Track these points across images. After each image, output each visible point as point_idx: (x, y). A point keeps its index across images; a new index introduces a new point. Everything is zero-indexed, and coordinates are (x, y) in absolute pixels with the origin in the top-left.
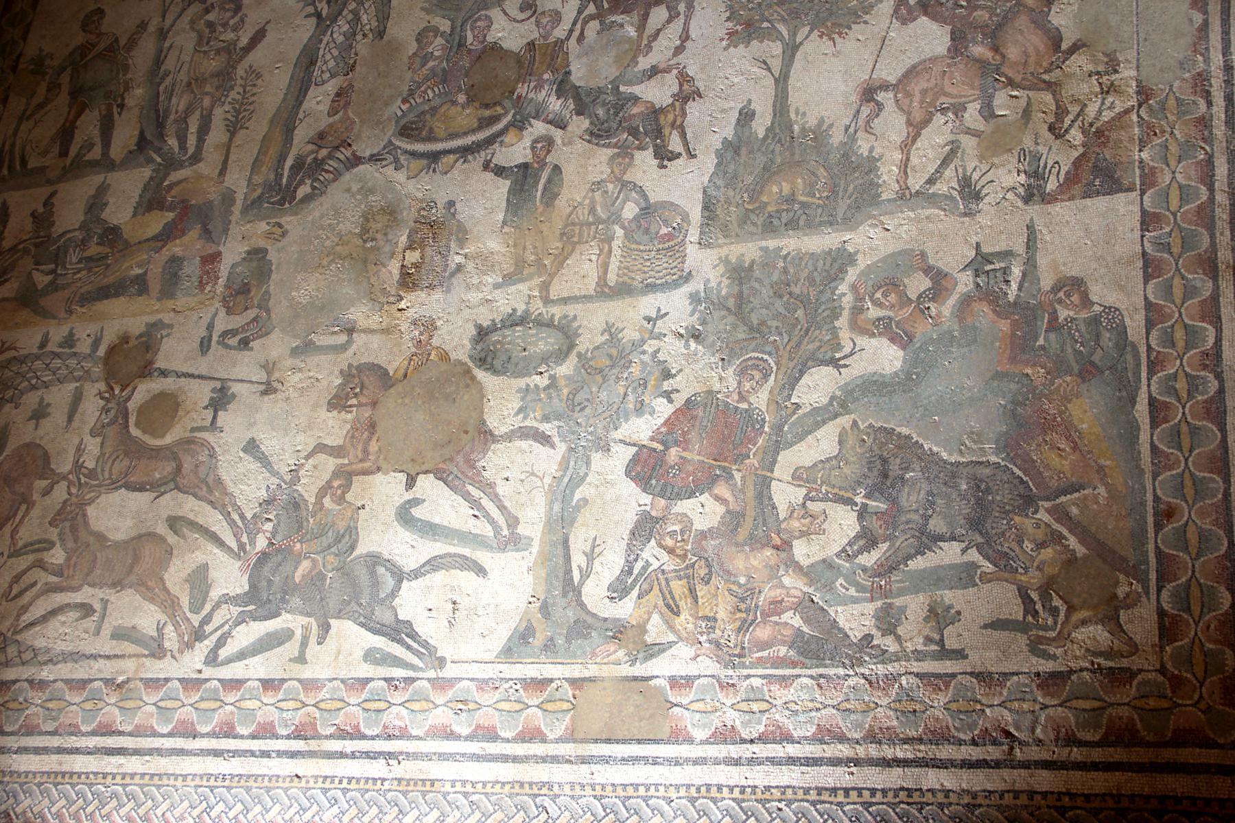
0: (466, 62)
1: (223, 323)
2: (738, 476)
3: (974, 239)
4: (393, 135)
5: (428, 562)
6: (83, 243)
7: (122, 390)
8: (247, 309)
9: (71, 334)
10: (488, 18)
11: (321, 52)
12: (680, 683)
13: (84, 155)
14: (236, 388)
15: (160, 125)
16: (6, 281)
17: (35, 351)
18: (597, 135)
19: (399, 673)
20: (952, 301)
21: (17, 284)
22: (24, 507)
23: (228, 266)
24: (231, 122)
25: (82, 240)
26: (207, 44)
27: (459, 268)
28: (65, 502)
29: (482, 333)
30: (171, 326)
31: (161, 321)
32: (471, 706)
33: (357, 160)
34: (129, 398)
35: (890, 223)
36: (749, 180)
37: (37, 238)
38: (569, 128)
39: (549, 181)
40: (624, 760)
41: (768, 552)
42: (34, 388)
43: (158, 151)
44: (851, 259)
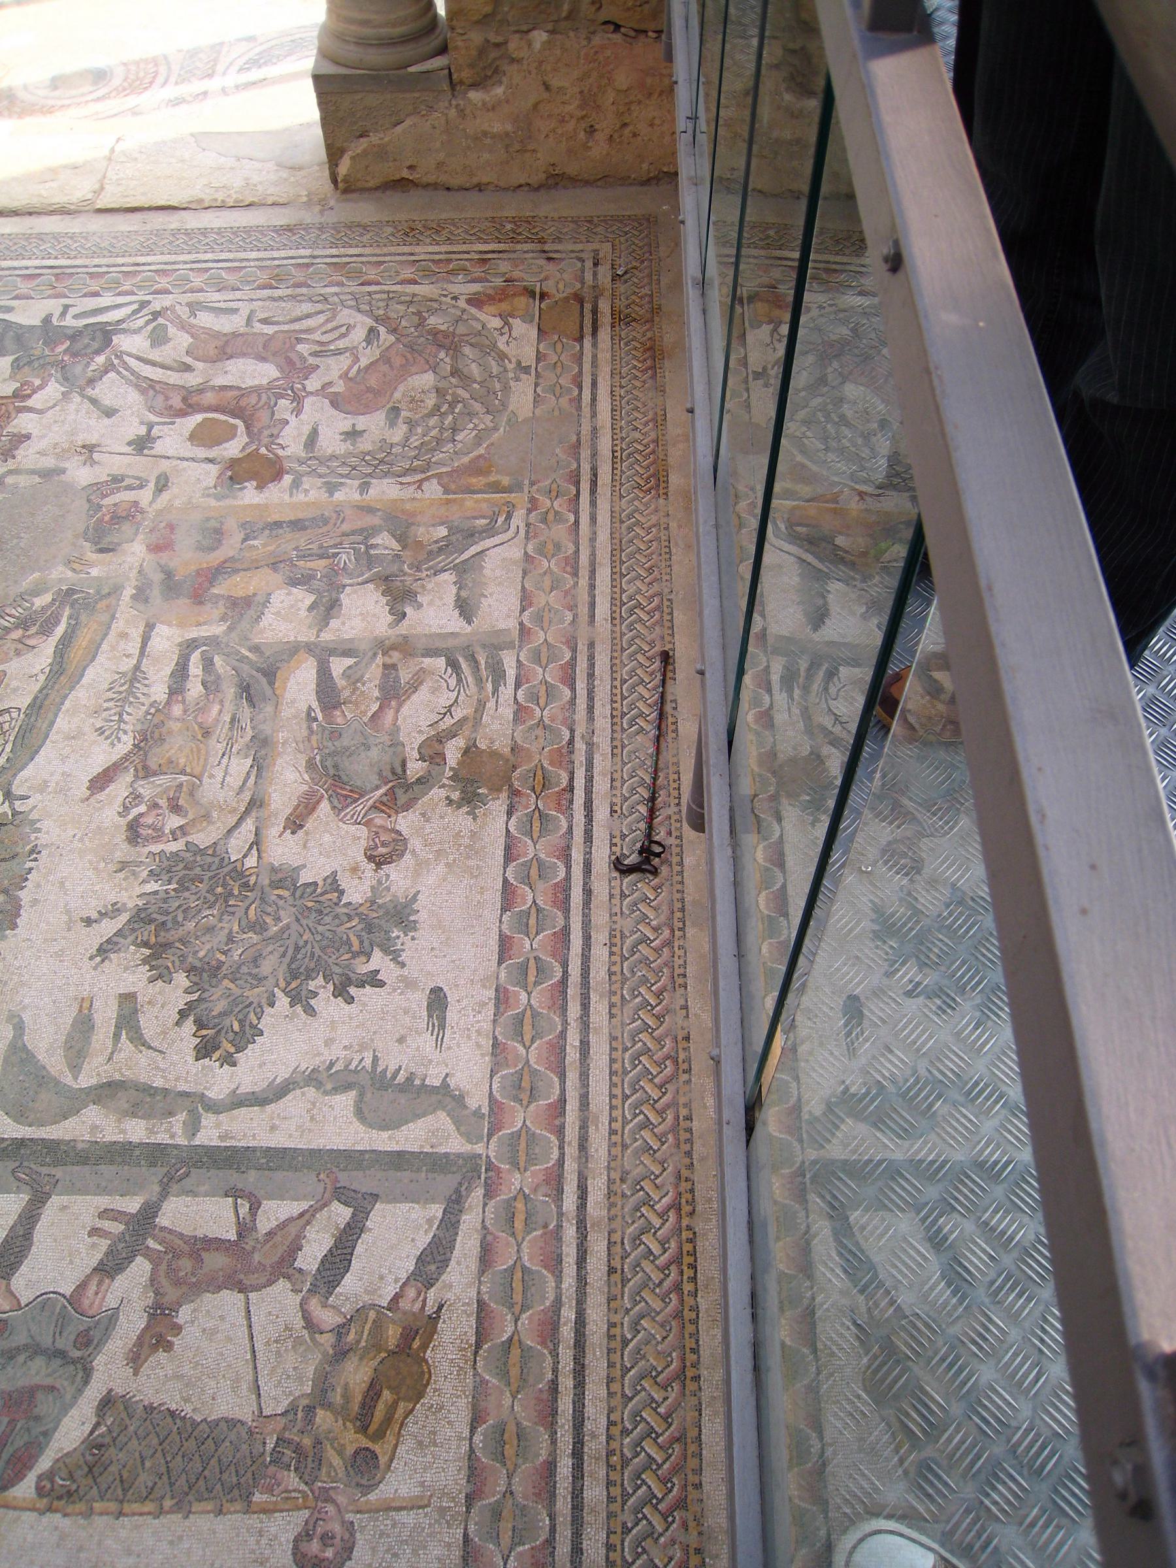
1: (145, 496)
6: (333, 573)
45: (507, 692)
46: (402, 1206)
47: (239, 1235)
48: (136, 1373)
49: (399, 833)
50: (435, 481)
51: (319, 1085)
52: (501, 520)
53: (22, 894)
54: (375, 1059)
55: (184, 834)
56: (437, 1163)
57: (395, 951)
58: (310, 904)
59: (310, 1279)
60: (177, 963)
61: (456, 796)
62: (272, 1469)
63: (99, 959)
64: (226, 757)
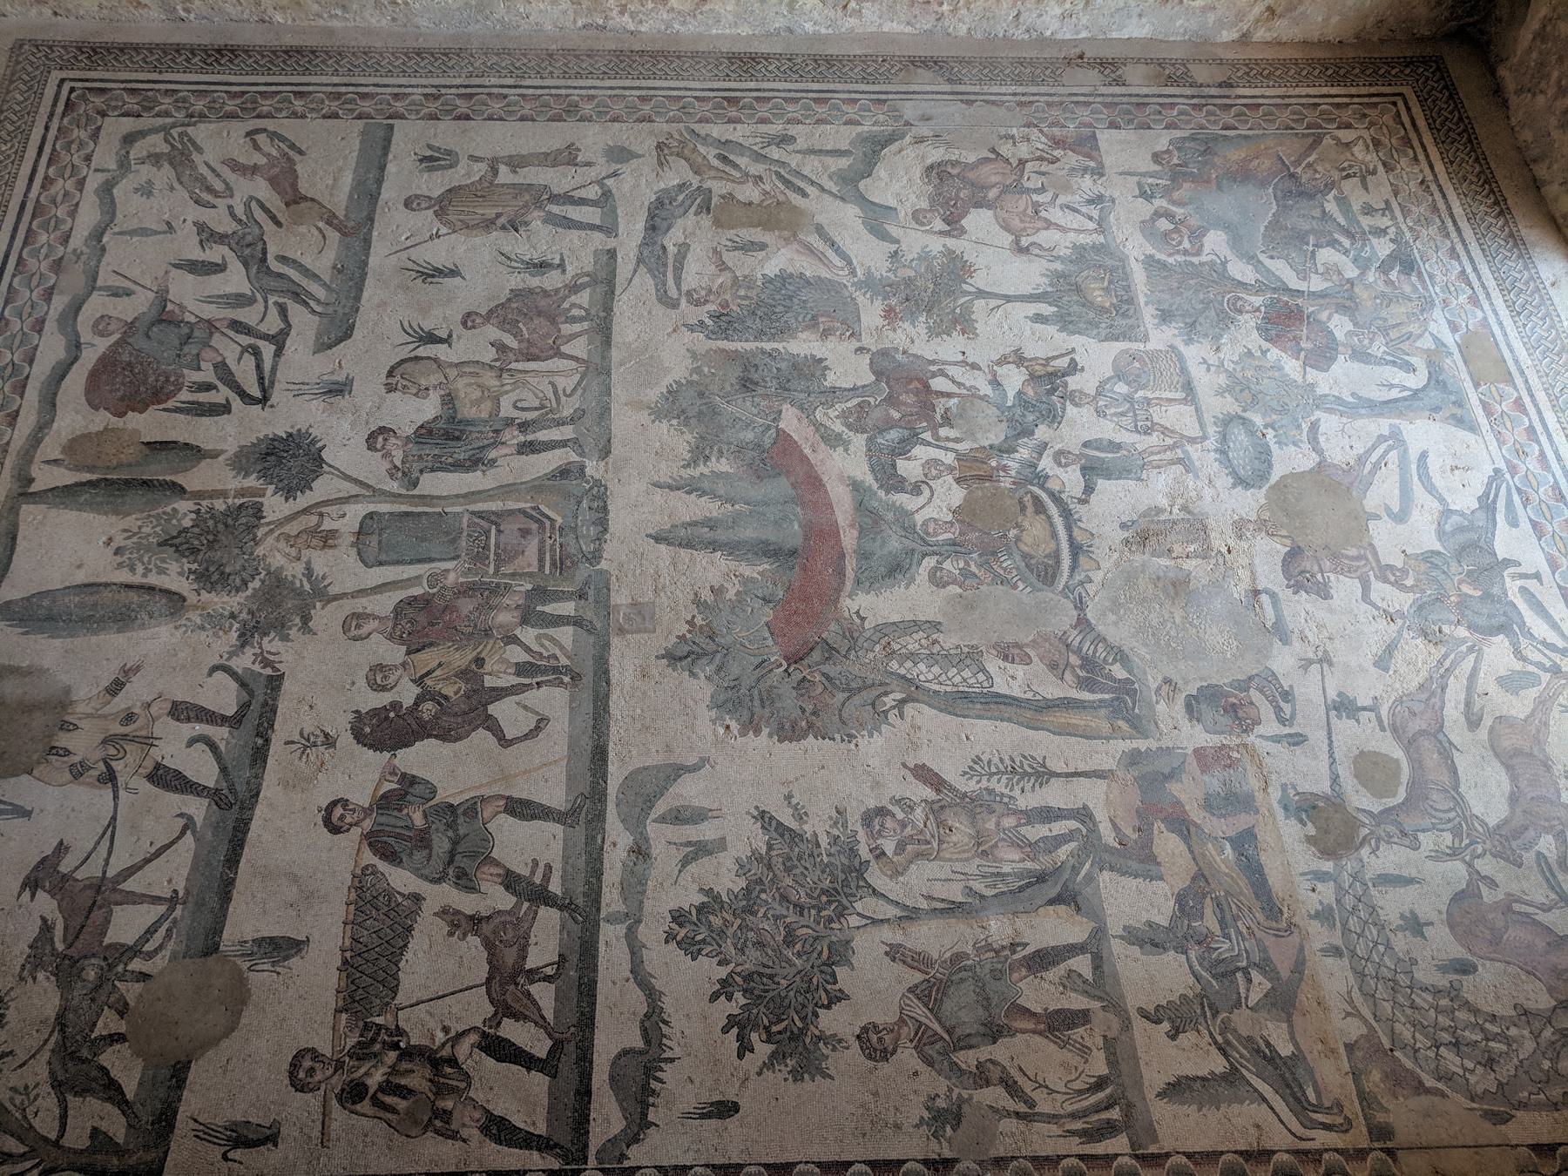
0: (973, 536)
1: (1270, 727)
2: (1311, 309)
3: (1130, 199)
4: (1053, 592)
5: (1430, 493)
7: (1364, 824)
8: (1252, 703)
9: (1317, 916)
10: (925, 523)
11: (949, 689)
12: (1454, 328)
13: (1085, 982)
14: (1332, 694)
15: (1041, 878)
16: (1268, 1044)
17: (1346, 961)
18: (1053, 417)
19: (1516, 498)
20: (1174, 209)
21: (1270, 1025)
22: (1516, 907)
23: (1208, 737)
24: (1036, 781)
25: (1199, 943)
26: (928, 843)
27: (1184, 508)
28: (1495, 856)
29: (1240, 481)
30: (1284, 787)
31: (1280, 802)
32: (1518, 446)
33: (1082, 623)
34: (1370, 813)
35: (1120, 238)
36: (1092, 315)
37: (1205, 1017)
38: (1047, 440)
39: (1097, 449)
40: (1512, 351)
41: (1356, 290)
42: (1388, 947)
43: (1075, 870)
44: (1151, 256)
45: (1075, 1146)
46: (546, 1100)
47: (530, 971)
48: (435, 914)
49: (894, 1052)
50: (1364, 1031)
51: (647, 1016)
52: (1320, 1117)
53: (811, 738)
54: (672, 1060)
55: (877, 857)
56: (581, 1123)
57: (773, 1064)
58: (815, 981)
59: (492, 1031)
60: (754, 878)
61: (941, 1103)
62: (361, 1024)
63: (756, 813)
64: (963, 877)
